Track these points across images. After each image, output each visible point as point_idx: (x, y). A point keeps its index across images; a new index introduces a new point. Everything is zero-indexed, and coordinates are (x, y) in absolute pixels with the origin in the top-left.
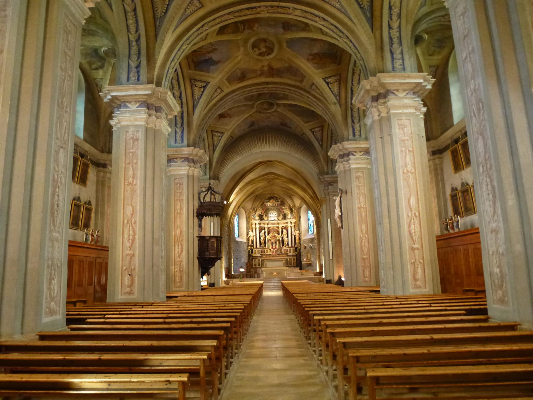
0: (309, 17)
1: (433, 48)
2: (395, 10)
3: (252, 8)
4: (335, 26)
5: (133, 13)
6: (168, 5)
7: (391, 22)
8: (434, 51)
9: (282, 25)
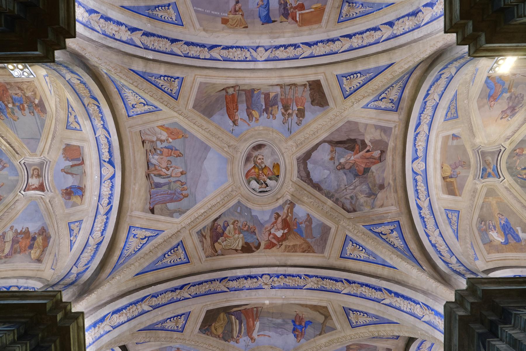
0: (328, 287)
2: (441, 248)
3: (251, 277)
4: (367, 285)
5: (95, 247)
6: (144, 244)
7: (442, 258)
9: (291, 326)
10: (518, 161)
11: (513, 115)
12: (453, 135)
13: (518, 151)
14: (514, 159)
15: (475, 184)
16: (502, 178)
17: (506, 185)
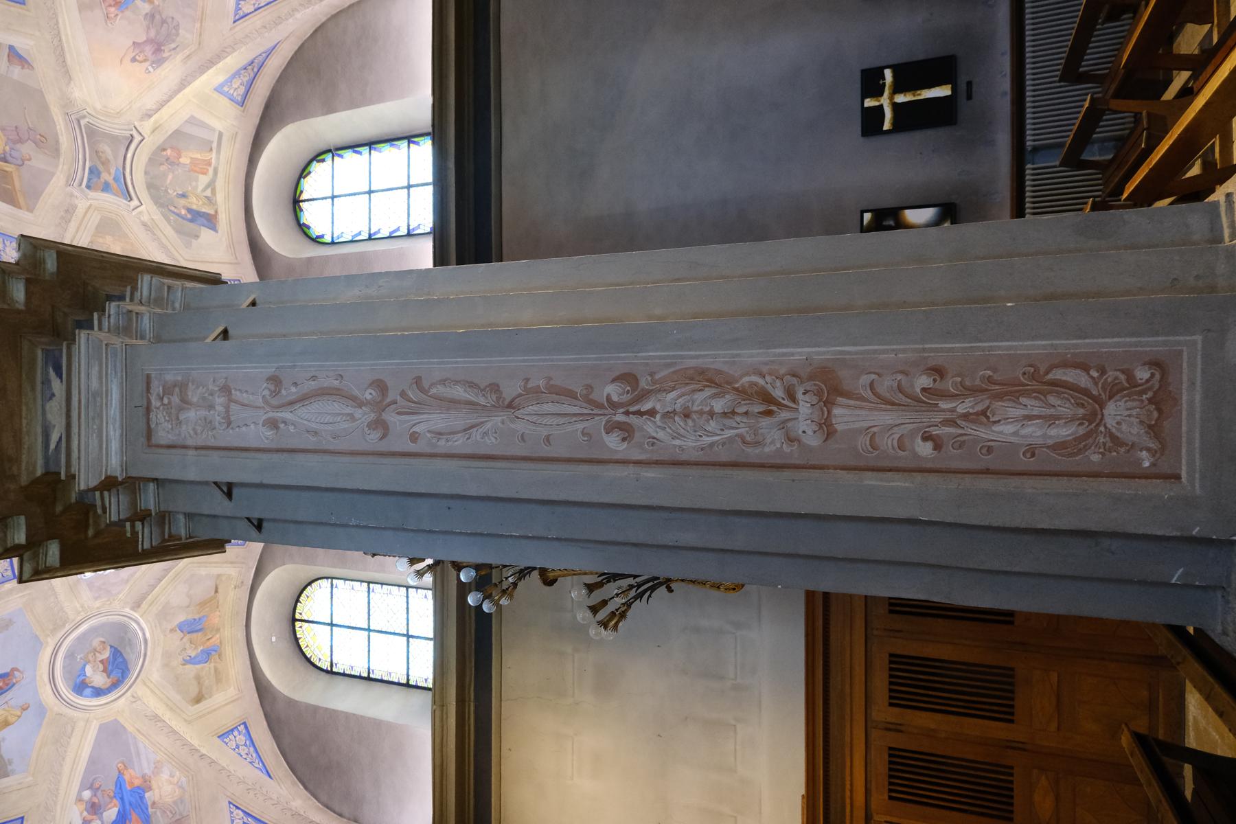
1: (191, 669)
8: (198, 678)
10: (170, 176)
11: (158, 62)
12: (11, 48)
13: (169, 152)
14: (162, 168)
15: (72, 195)
16: (135, 202)
17: (145, 218)
